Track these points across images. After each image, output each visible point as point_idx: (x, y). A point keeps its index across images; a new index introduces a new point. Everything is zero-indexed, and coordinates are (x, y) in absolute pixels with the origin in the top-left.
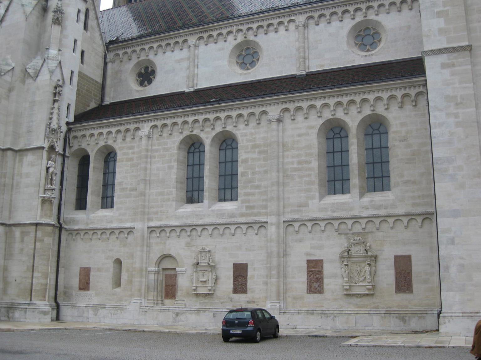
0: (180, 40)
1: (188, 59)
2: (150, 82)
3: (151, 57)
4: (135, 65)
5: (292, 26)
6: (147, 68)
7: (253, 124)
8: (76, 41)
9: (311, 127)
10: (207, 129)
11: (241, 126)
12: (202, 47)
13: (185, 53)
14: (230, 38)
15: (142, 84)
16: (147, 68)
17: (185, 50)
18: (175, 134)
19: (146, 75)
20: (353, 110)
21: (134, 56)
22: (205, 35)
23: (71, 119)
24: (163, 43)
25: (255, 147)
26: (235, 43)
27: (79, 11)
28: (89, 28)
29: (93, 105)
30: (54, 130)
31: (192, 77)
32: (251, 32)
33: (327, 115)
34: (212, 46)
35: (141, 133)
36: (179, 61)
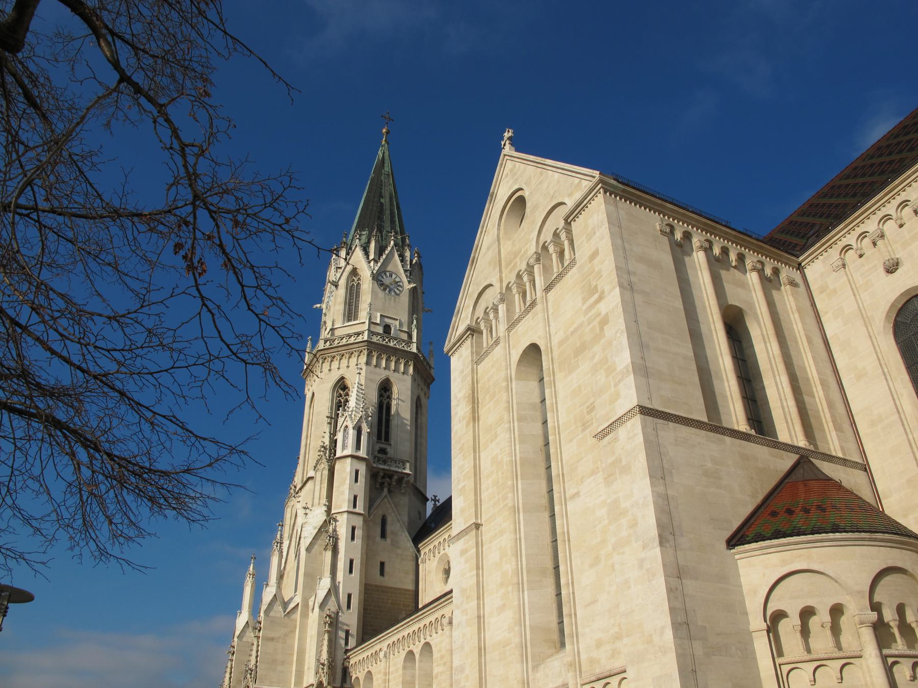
4: (438, 562)
8: (351, 562)
10: (417, 643)
18: (401, 651)
25: (442, 657)
27: (353, 529)
30: (323, 664)
35: (382, 654)
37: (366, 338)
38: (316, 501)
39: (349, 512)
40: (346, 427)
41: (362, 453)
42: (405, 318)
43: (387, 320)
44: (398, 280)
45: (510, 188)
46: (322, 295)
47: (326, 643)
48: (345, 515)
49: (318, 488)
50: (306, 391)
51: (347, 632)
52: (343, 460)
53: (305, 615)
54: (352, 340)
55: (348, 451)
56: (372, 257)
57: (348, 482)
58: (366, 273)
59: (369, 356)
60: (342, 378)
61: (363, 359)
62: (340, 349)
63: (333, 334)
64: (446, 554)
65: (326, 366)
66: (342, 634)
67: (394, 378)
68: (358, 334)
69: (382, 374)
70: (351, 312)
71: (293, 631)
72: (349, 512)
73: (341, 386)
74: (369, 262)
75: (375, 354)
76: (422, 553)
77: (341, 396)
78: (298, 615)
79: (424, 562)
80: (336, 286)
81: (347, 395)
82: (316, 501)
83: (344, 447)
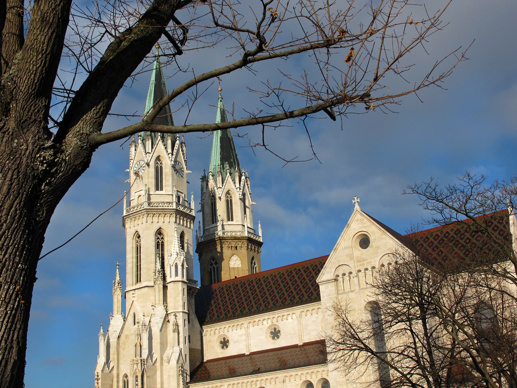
0: (240, 323)
1: (245, 335)
2: (227, 347)
3: (226, 333)
4: (218, 338)
5: (294, 316)
6: (224, 339)
7: (273, 383)
9: (297, 385)
11: (268, 384)
12: (251, 328)
13: (243, 331)
14: (265, 322)
15: (223, 348)
16: (224, 339)
17: (243, 329)
19: (225, 343)
20: (314, 376)
21: (217, 331)
22: (252, 321)
23: (188, 380)
24: (231, 325)
26: (267, 325)
28: (190, 321)
29: (198, 364)
31: (248, 346)
32: (275, 319)
33: (304, 379)
34: (256, 327)
36: (240, 336)
37: (174, 207)
38: (157, 302)
39: (183, 312)
40: (176, 263)
41: (185, 279)
42: (186, 193)
43: (179, 193)
44: (181, 167)
45: (360, 228)
46: (129, 164)
47: (181, 380)
48: (181, 314)
49: (157, 294)
50: (127, 226)
51: (186, 373)
52: (176, 283)
53: (162, 364)
54: (166, 206)
55: (179, 278)
56: (170, 151)
57: (181, 295)
58: (167, 163)
59: (176, 218)
60: (160, 228)
61: (174, 220)
62: (159, 210)
63: (149, 199)
64: (226, 336)
65: (150, 219)
66: (185, 375)
67: (186, 231)
68: (169, 203)
69: (182, 228)
70: (159, 186)
71: (156, 372)
72: (183, 312)
73: (159, 232)
74: (169, 154)
75: (178, 216)
76: (205, 330)
77: (158, 238)
78: (158, 364)
79: (206, 335)
80: (148, 165)
81: (162, 238)
82: (157, 302)
83: (177, 275)
